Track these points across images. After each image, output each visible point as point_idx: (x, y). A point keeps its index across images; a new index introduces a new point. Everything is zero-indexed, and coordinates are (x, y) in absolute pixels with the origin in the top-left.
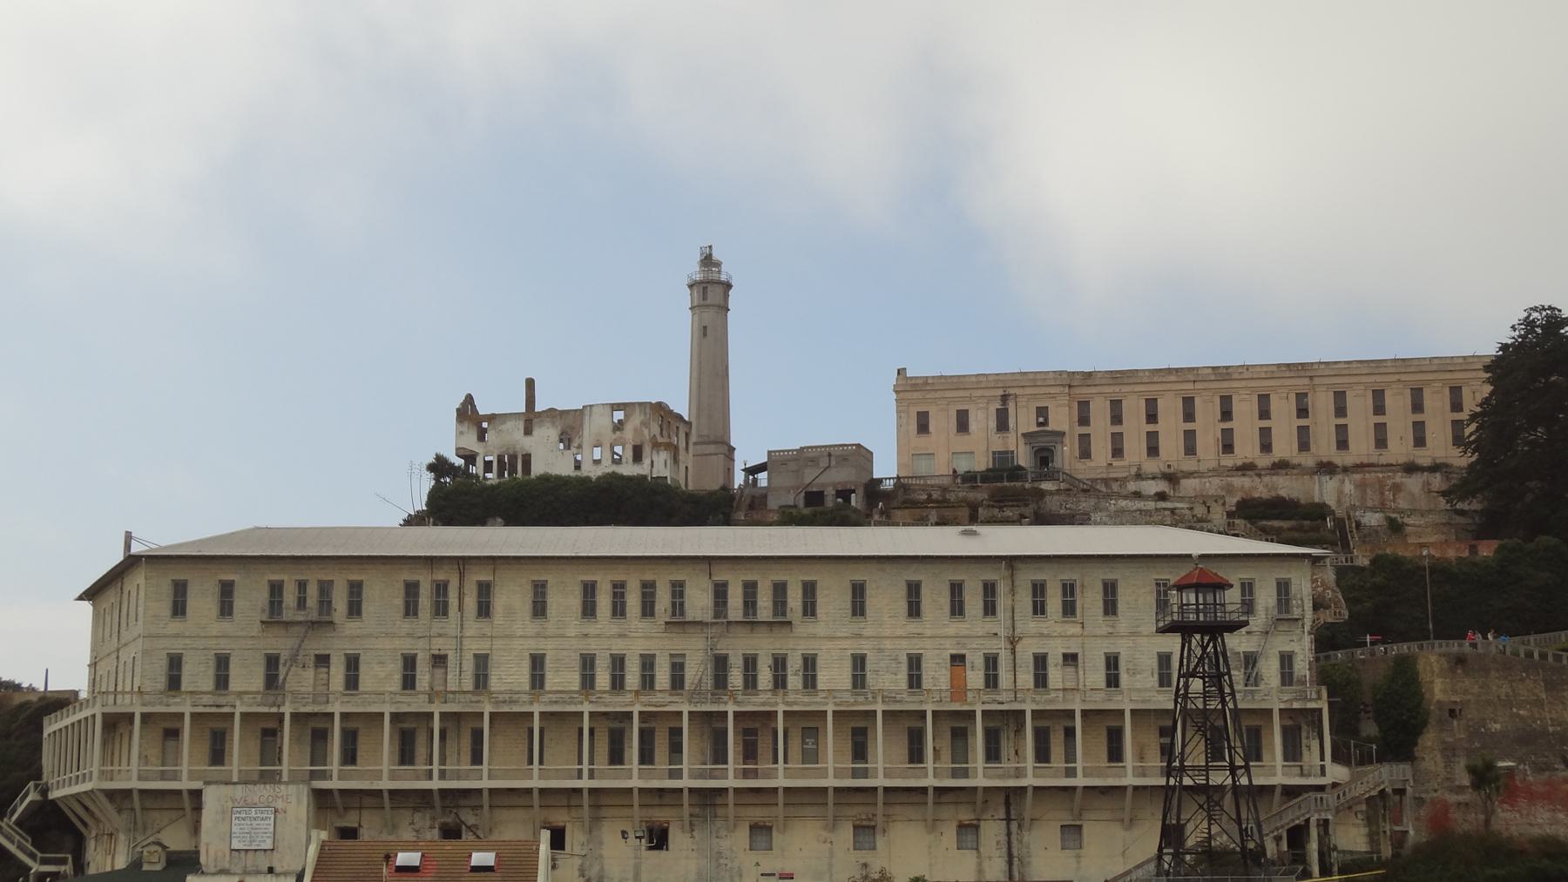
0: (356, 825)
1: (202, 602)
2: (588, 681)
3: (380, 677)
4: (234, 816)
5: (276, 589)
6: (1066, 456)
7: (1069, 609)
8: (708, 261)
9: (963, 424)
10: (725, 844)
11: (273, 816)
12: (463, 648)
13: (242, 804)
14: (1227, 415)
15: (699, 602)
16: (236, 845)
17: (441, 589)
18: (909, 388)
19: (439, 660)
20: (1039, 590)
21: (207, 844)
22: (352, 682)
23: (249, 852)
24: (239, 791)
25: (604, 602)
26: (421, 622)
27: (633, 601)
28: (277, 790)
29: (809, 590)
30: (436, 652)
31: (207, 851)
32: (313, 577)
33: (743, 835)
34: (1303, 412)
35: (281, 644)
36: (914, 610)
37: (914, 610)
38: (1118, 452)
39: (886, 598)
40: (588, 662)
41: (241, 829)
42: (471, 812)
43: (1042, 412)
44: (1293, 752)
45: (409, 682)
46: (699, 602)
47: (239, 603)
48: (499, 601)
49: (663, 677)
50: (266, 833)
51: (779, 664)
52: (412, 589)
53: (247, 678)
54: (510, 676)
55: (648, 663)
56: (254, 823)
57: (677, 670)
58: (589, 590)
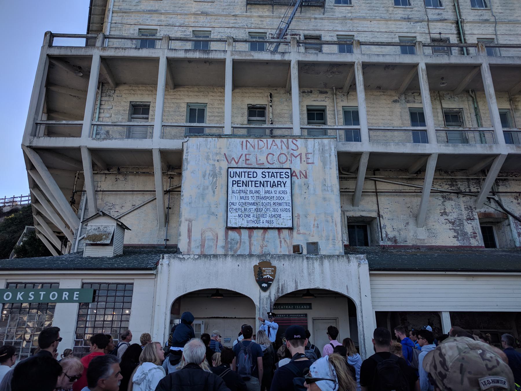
0: (374, 215)
4: (230, 180)
11: (288, 181)
12: (466, 33)
13: (242, 164)
16: (234, 221)
21: (190, 221)
23: (255, 231)
26: (416, 9)
28: (292, 146)
30: (437, 36)
31: (189, 231)
41: (241, 198)
42: (515, 201)
50: (280, 204)
56: (262, 189)
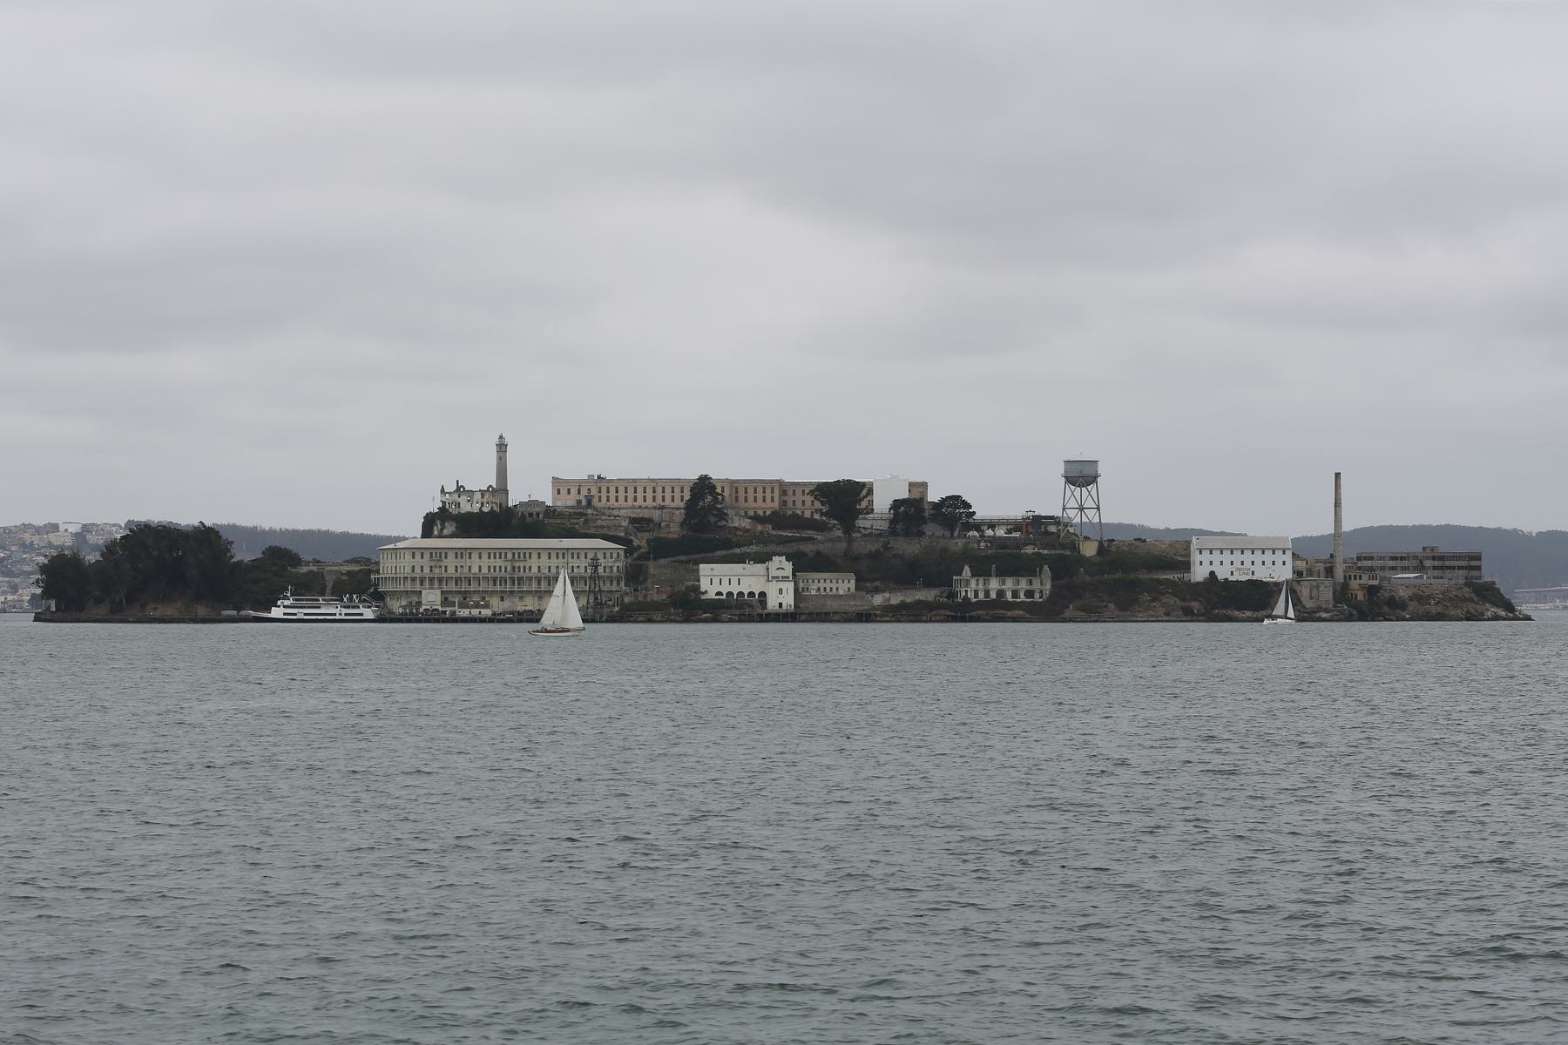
1: (418, 556)
2: (489, 571)
3: (451, 570)
5: (431, 553)
6: (595, 501)
7: (578, 557)
8: (501, 437)
9: (569, 493)
10: (514, 600)
14: (635, 492)
15: (510, 556)
17: (462, 554)
18: (556, 481)
19: (462, 567)
20: (573, 554)
22: (446, 571)
24: (428, 591)
25: (492, 556)
27: (498, 556)
29: (530, 554)
32: (438, 551)
33: (518, 599)
34: (654, 492)
35: (433, 564)
36: (550, 558)
37: (550, 558)
38: (608, 501)
39: (544, 556)
40: (489, 567)
43: (589, 490)
44: (618, 584)
45: (456, 571)
46: (510, 556)
47: (425, 556)
48: (473, 556)
49: (503, 570)
51: (525, 567)
52: (456, 554)
53: (427, 570)
54: (475, 570)
55: (500, 567)
57: (506, 568)
58: (489, 554)
